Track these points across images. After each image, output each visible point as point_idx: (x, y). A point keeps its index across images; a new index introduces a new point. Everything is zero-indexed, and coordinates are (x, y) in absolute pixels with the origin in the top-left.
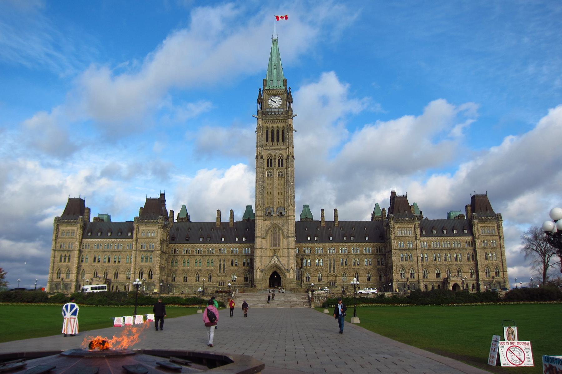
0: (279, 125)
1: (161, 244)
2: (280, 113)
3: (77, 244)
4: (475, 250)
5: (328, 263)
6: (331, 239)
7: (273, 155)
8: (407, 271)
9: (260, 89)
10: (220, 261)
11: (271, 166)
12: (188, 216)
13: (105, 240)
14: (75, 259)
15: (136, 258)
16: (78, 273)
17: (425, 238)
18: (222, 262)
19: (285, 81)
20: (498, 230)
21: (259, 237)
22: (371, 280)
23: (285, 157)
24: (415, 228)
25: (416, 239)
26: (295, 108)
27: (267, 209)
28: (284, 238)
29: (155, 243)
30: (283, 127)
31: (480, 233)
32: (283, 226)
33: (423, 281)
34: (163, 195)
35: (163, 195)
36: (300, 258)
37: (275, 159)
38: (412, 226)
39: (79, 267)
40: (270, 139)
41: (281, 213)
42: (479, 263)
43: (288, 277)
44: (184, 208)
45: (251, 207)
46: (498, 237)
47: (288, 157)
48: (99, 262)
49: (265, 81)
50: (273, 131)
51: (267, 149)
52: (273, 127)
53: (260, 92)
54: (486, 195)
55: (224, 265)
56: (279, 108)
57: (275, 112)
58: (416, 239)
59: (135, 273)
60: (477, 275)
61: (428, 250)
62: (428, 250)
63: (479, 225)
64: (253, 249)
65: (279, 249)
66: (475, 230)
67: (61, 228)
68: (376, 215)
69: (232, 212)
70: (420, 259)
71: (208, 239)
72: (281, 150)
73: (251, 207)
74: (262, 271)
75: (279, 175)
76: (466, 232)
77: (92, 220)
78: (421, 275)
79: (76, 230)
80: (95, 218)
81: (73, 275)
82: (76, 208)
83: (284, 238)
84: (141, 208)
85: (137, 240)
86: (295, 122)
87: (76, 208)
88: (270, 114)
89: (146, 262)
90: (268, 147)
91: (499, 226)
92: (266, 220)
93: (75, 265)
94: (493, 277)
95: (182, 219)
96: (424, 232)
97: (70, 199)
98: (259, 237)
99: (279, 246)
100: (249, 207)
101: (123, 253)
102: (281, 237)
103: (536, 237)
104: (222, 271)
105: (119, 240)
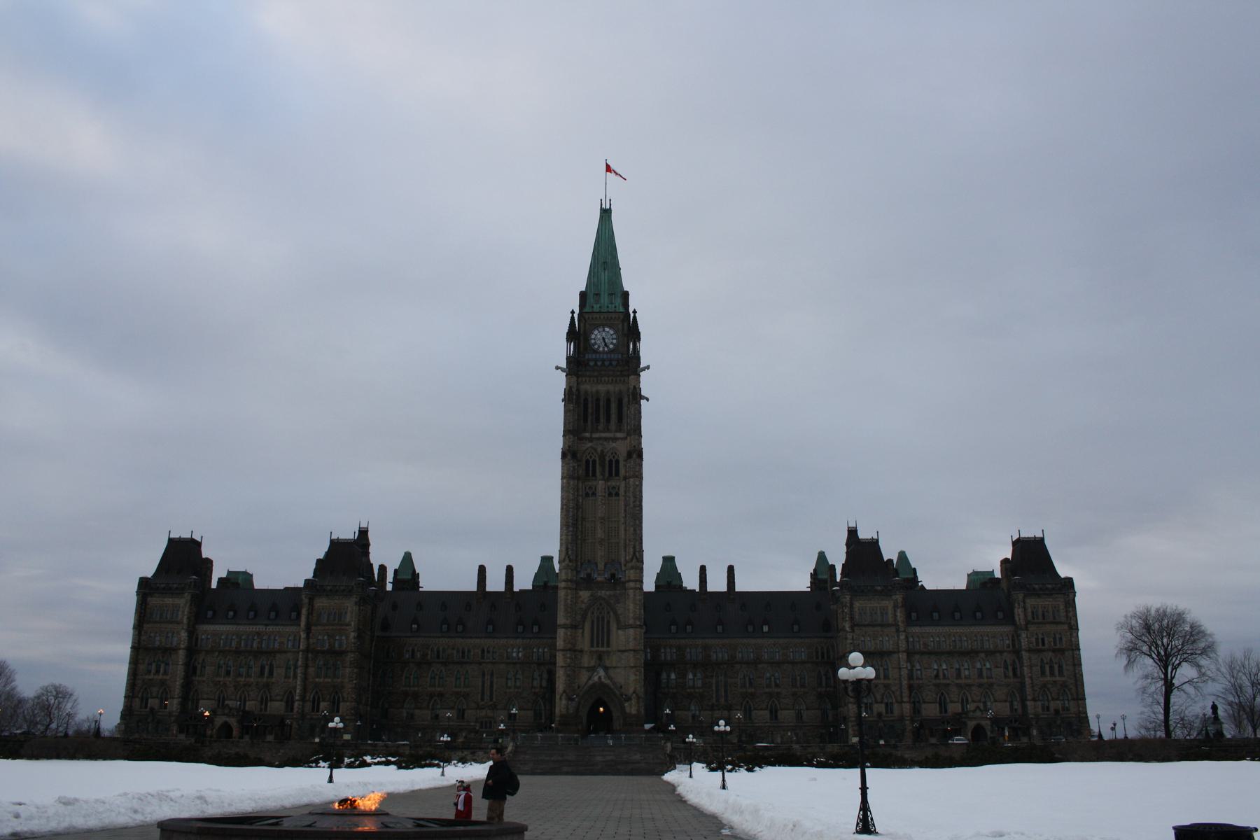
0: (611, 388)
1: (359, 637)
2: (614, 363)
3: (184, 635)
4: (1017, 653)
5: (714, 681)
7: (599, 450)
8: (879, 697)
9: (573, 312)
10: (484, 675)
11: (594, 474)
12: (415, 576)
13: (241, 628)
14: (180, 670)
15: (306, 666)
16: (185, 698)
17: (916, 629)
18: (487, 677)
19: (626, 295)
20: (1067, 612)
21: (565, 626)
22: (805, 717)
23: (622, 455)
24: (895, 607)
25: (898, 631)
26: (647, 350)
28: (618, 629)
29: (347, 638)
30: (620, 392)
31: (1030, 618)
33: (912, 721)
34: (363, 533)
35: (363, 533)
36: (653, 670)
37: (602, 456)
38: (888, 604)
39: (188, 685)
41: (613, 576)
42: (1028, 681)
43: (628, 710)
44: (408, 558)
45: (551, 558)
46: (1066, 627)
47: (629, 455)
48: (228, 673)
49: (583, 296)
50: (598, 400)
51: (586, 438)
52: (597, 392)
54: (1042, 539)
55: (492, 683)
56: (611, 351)
57: (603, 361)
58: (898, 631)
59: (303, 699)
60: (1024, 707)
61: (922, 653)
62: (922, 653)
63: (1028, 601)
64: (553, 647)
65: (608, 652)
66: (1019, 611)
67: (154, 601)
68: (820, 577)
69: (510, 570)
70: (904, 673)
71: (460, 628)
72: (615, 439)
73: (551, 558)
74: (570, 699)
75: (610, 495)
76: (1000, 615)
77: (214, 585)
78: (907, 708)
79: (182, 605)
80: (220, 580)
81: (175, 701)
82: (183, 557)
83: (618, 629)
84: (318, 561)
86: (647, 383)
87: (183, 557)
88: (592, 364)
89: (326, 677)
90: (587, 435)
91: (1071, 604)
93: (179, 682)
94: (1057, 712)
95: (404, 581)
96: (914, 615)
97: (171, 540)
99: (608, 646)
100: (547, 560)
101: (278, 656)
102: (614, 626)
103: (1147, 627)
104: (487, 697)
105: (270, 629)
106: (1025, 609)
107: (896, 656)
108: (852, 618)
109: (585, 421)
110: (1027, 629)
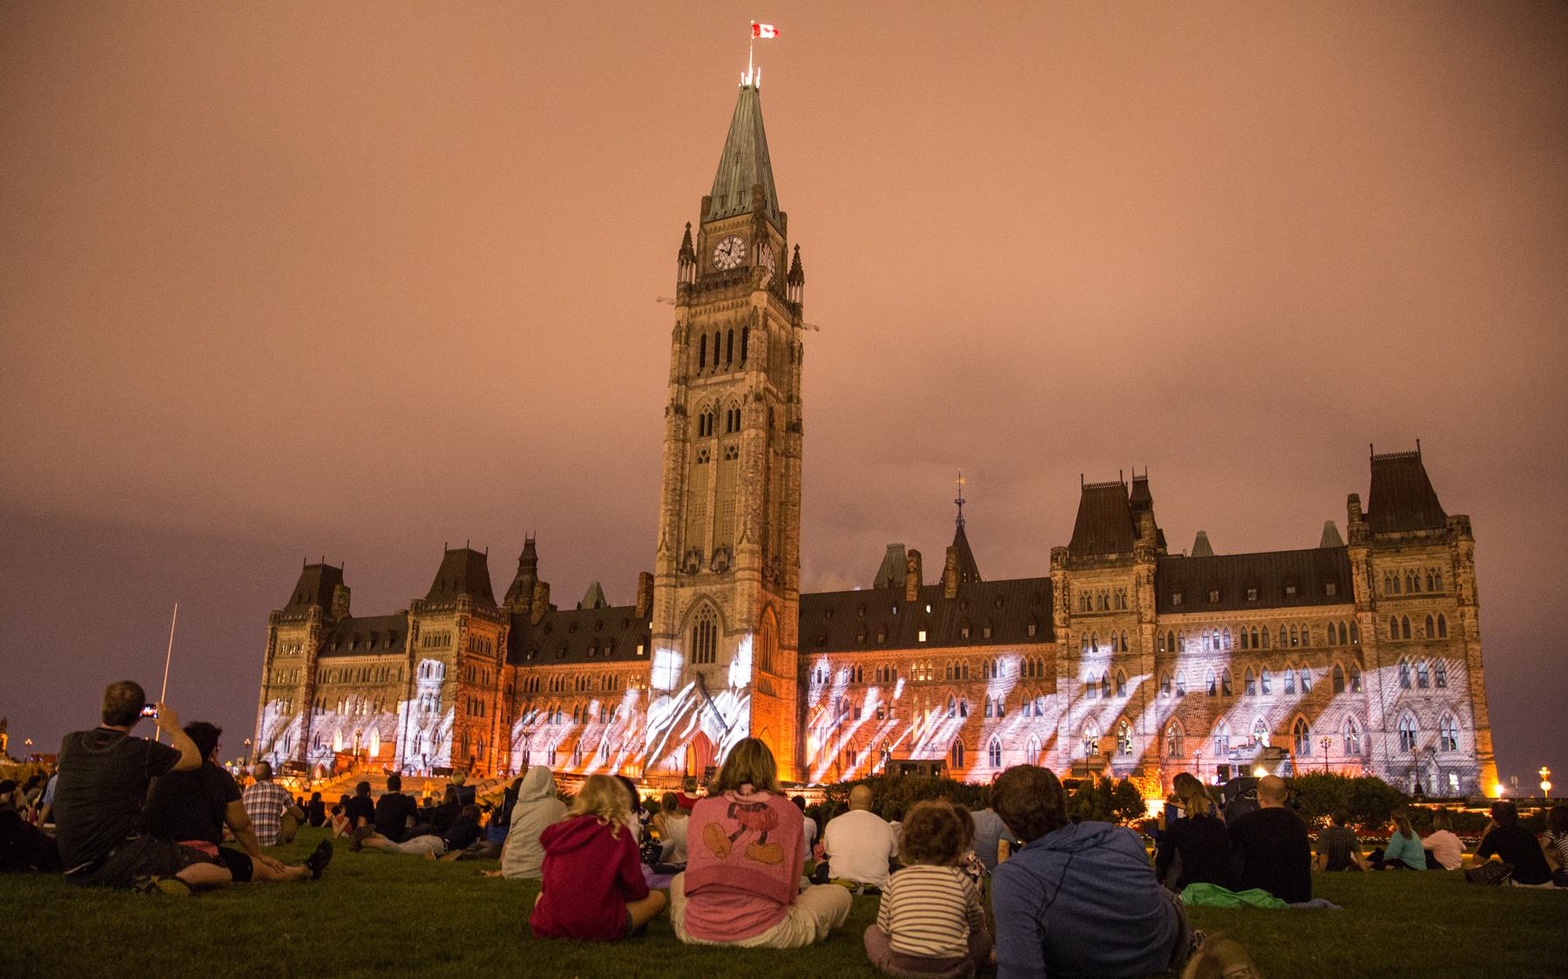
6: (922, 636)
9: (689, 225)
21: (659, 635)
24: (1138, 584)
27: (688, 554)
31: (1381, 587)
32: (725, 600)
38: (1125, 581)
40: (709, 358)
41: (721, 563)
46: (1453, 601)
49: (707, 201)
50: (718, 334)
53: (688, 235)
58: (1140, 622)
66: (1359, 580)
85: (412, 657)
90: (701, 381)
92: (682, 585)
98: (659, 635)
102: (720, 632)
106: (1370, 577)
107: (1138, 661)
108: (1067, 607)
109: (702, 364)
110: (1373, 610)
